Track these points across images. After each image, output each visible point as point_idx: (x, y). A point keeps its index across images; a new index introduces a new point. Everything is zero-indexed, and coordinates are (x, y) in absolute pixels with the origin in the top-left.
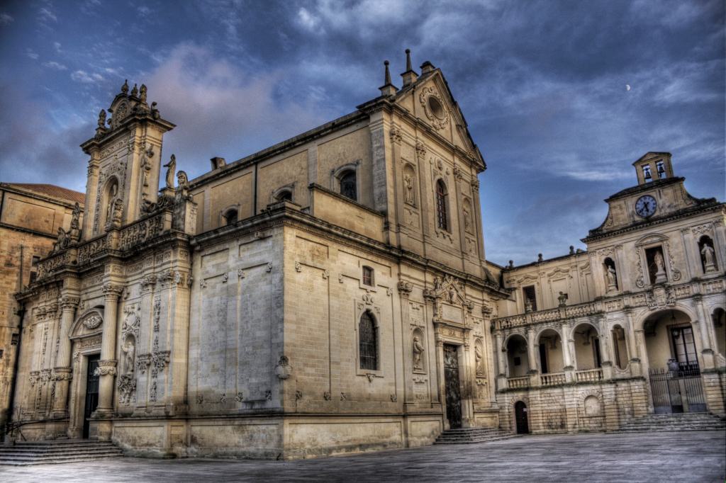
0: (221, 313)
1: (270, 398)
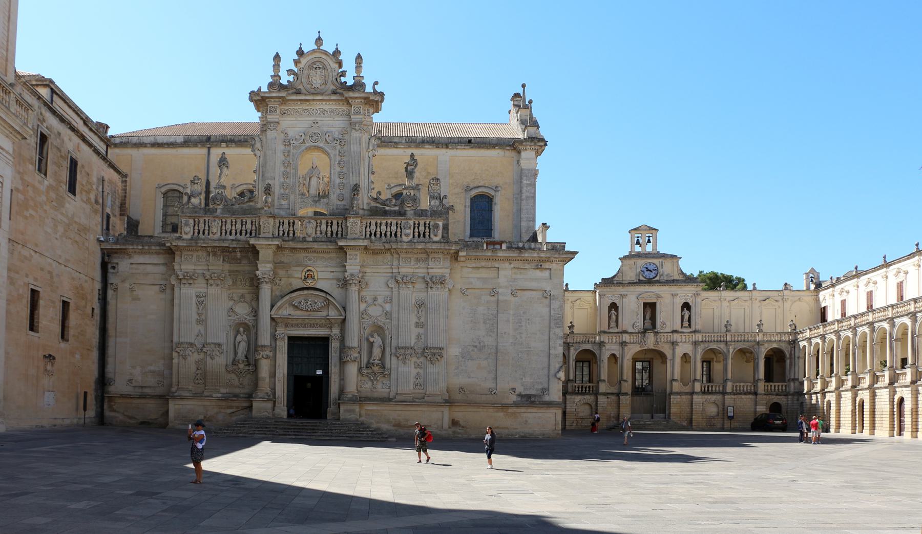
1: (548, 394)
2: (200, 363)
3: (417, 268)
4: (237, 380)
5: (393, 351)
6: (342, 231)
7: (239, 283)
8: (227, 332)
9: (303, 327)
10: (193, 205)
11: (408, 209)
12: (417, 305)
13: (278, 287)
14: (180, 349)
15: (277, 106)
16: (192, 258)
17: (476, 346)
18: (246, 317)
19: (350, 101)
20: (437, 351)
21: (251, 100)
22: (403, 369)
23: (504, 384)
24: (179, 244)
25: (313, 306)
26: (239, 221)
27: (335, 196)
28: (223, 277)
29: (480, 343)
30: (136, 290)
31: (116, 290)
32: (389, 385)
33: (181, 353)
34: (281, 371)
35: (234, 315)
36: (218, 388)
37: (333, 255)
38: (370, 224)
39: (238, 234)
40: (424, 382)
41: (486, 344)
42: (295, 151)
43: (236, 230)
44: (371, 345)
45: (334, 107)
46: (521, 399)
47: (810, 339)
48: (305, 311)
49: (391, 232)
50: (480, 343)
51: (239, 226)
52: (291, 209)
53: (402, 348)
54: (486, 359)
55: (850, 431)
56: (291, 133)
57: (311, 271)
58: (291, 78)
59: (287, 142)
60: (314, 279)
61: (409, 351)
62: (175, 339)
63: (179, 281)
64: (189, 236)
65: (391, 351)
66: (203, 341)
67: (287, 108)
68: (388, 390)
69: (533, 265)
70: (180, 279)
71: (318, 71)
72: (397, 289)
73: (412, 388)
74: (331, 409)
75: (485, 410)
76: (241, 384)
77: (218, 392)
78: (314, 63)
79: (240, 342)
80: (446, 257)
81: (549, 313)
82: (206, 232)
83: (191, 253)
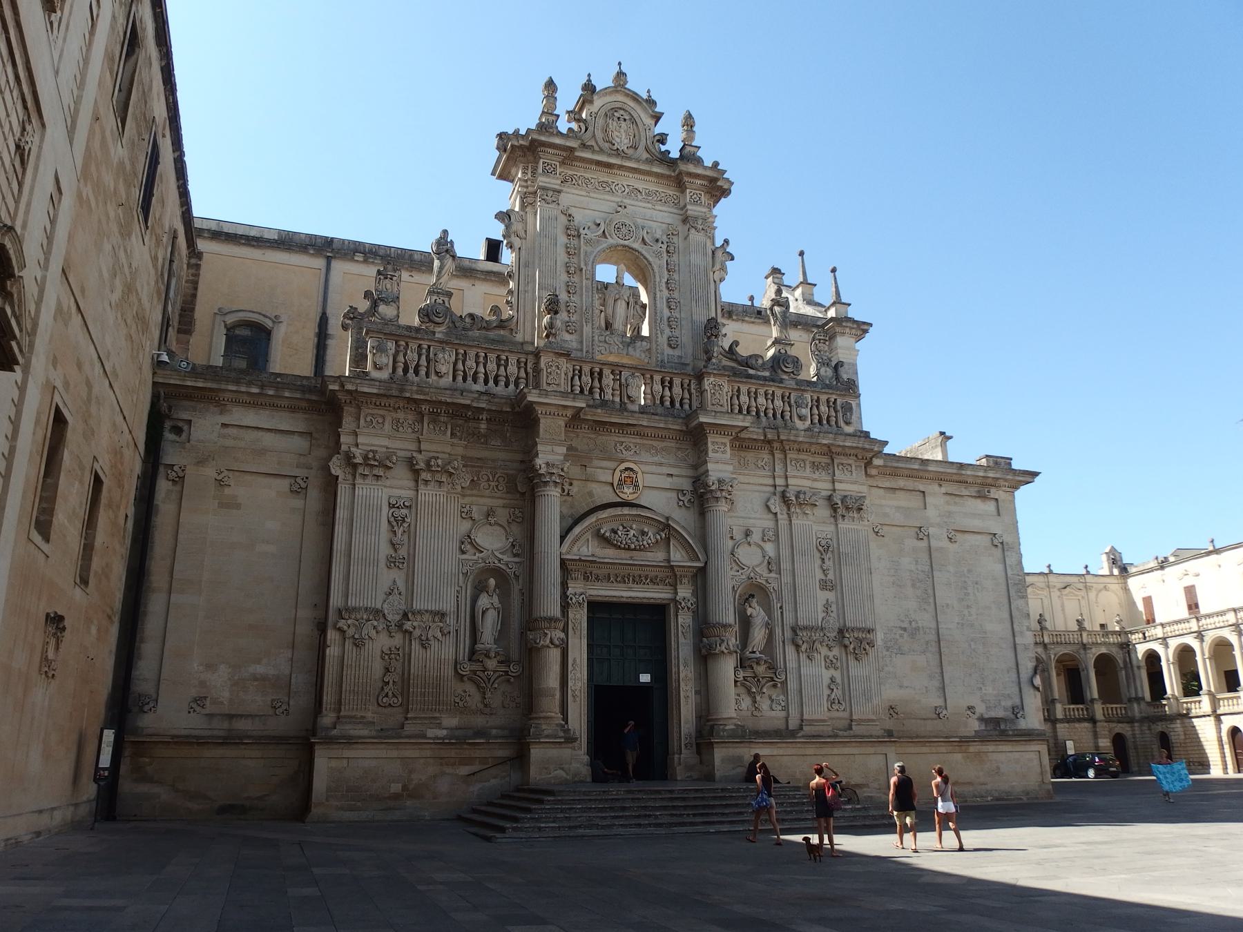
0: (918, 584)
2: (393, 656)
3: (815, 480)
4: (477, 697)
5: (788, 634)
6: (690, 400)
7: (484, 484)
8: (457, 588)
9: (620, 582)
10: (382, 319)
11: (785, 377)
12: (820, 548)
14: (349, 622)
15: (558, 164)
16: (383, 423)
17: (905, 629)
18: (500, 556)
19: (686, 179)
20: (864, 636)
21: (502, 148)
22: (808, 670)
23: (959, 698)
24: (360, 389)
25: (640, 539)
26: (492, 357)
27: (665, 337)
28: (454, 468)
29: (910, 622)
30: (232, 484)
31: (179, 480)
32: (783, 704)
33: (350, 632)
34: (578, 675)
35: (473, 551)
36: (438, 715)
37: (670, 444)
38: (739, 390)
39: (491, 382)
40: (844, 694)
41: (920, 625)
42: (589, 249)
43: (486, 374)
44: (746, 623)
45: (653, 188)
46: (986, 726)
47: (1164, 639)
48: (624, 549)
49: (774, 409)
50: (910, 622)
51: (492, 366)
52: (584, 350)
53: (805, 628)
54: (924, 652)
55: (1222, 771)
56: (579, 217)
57: (631, 470)
58: (574, 126)
59: (573, 232)
60: (636, 486)
61: (817, 636)
62: (336, 600)
63: (349, 470)
64: (384, 375)
65: (783, 634)
66: (404, 607)
67: (570, 172)
68: (783, 714)
69: (973, 491)
70: (355, 466)
71: (623, 124)
72: (786, 516)
73: (826, 709)
74: (683, 758)
75: (934, 750)
76: (486, 706)
77: (439, 726)
78: (615, 110)
79: (487, 609)
80: (858, 464)
81: (1003, 574)
82: (423, 372)
83: (381, 412)
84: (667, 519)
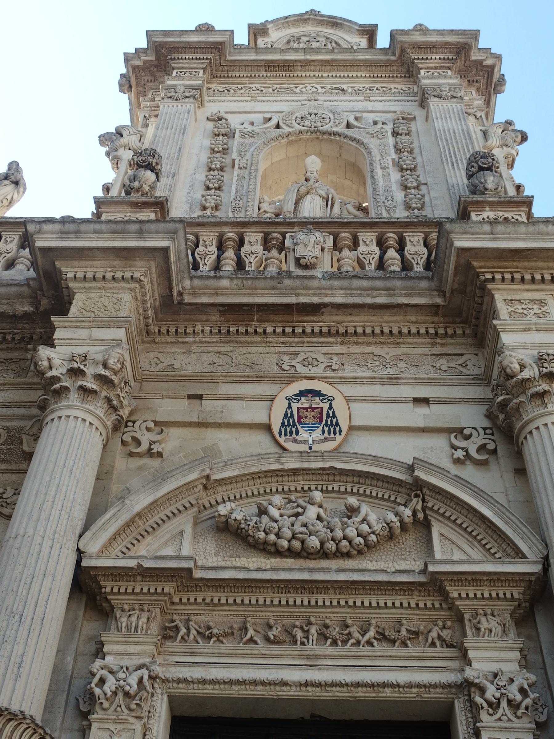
9: (276, 642)
13: (147, 461)
57: (316, 393)
84: (411, 468)
